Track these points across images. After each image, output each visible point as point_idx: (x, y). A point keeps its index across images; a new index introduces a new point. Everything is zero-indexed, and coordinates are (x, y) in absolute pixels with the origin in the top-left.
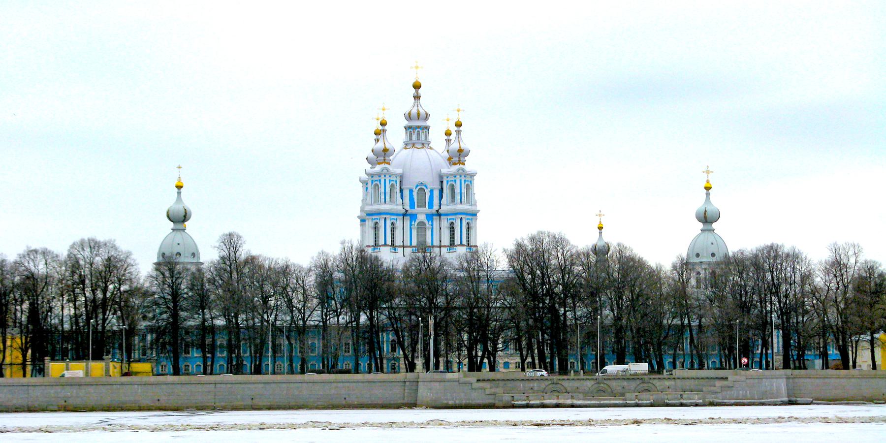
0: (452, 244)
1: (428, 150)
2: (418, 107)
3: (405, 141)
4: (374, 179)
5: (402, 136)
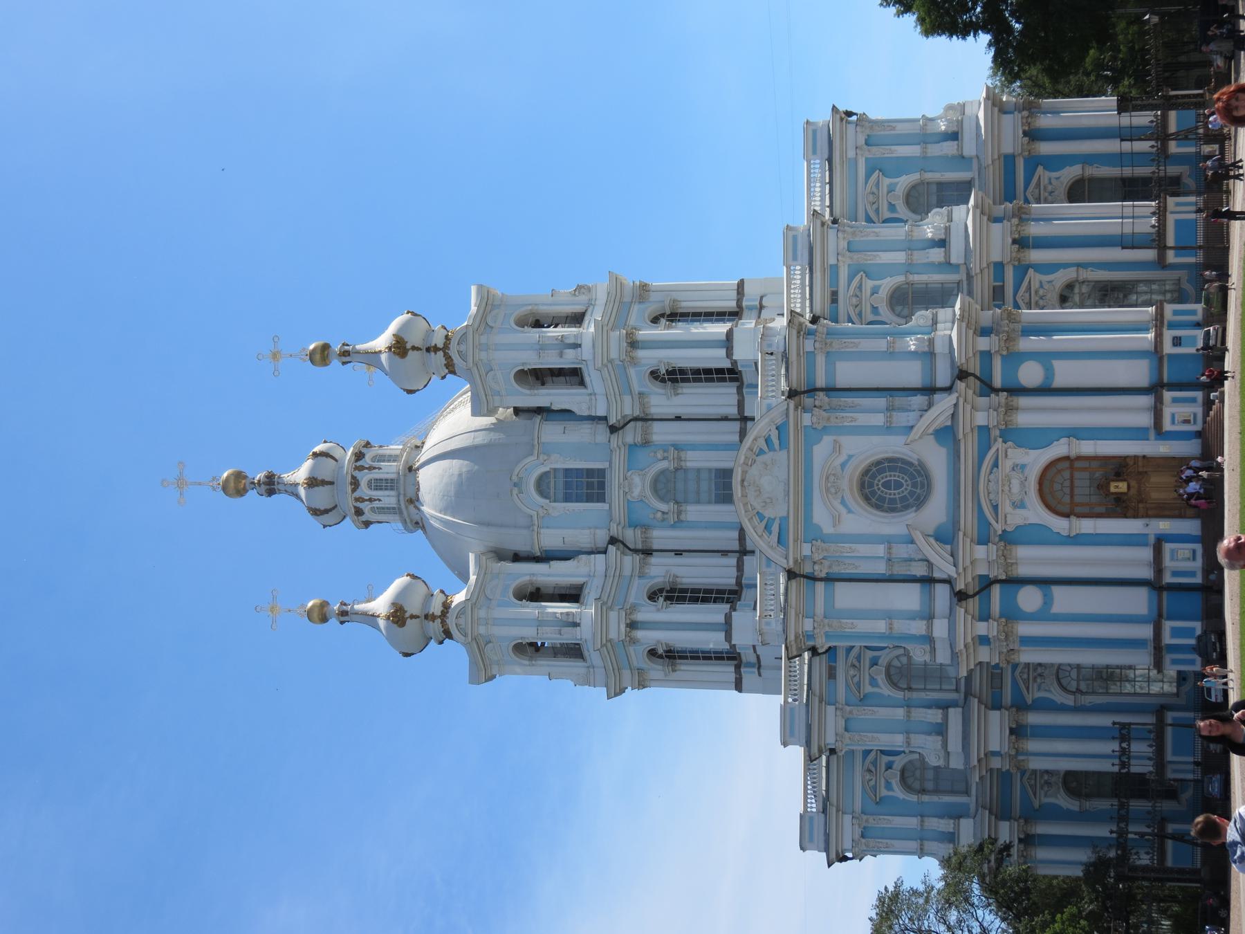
1: (424, 455)
3: (400, 526)
5: (388, 532)
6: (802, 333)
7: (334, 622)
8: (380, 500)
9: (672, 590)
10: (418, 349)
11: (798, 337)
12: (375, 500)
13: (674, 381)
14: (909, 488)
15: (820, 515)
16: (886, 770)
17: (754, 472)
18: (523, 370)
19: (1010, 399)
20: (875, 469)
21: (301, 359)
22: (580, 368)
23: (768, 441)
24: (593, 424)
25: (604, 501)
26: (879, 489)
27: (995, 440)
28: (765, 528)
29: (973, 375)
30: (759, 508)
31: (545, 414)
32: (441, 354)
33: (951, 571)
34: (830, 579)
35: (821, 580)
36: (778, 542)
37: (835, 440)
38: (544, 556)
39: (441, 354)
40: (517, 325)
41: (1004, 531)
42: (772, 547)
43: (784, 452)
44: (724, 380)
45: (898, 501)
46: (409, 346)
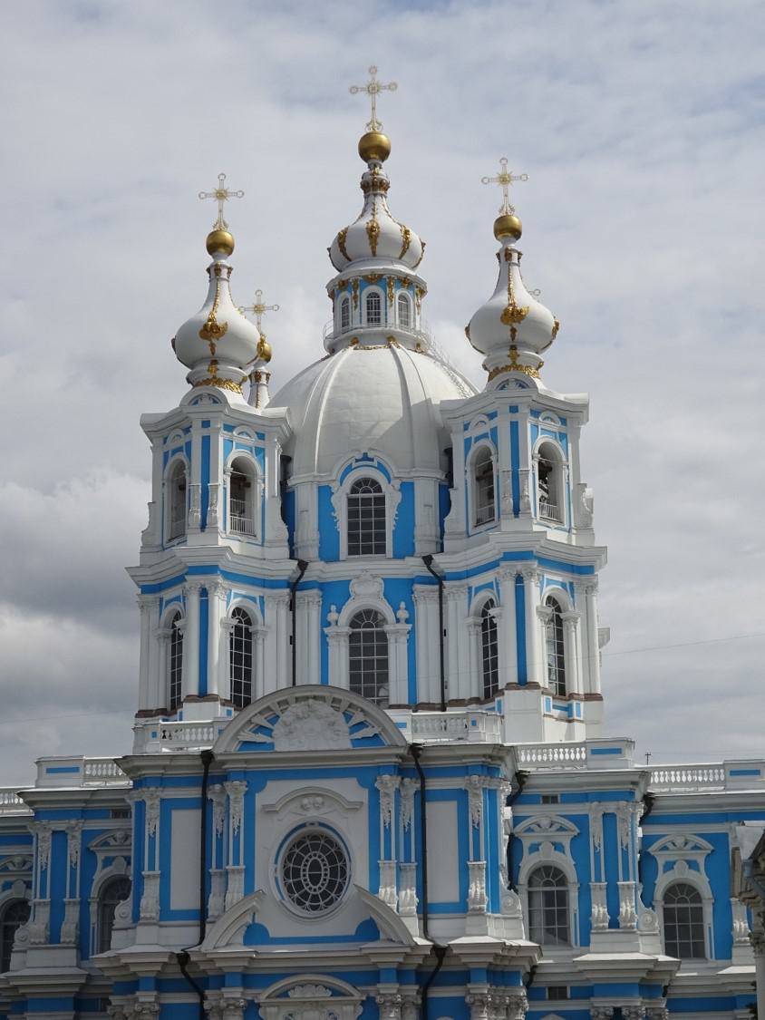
0: (491, 691)
2: (373, 215)
4: (171, 445)
6: (489, 760)
7: (209, 260)
8: (356, 307)
9: (249, 635)
10: (513, 337)
11: (484, 756)
12: (356, 302)
13: (484, 626)
14: (312, 892)
15: (273, 792)
16: (25, 882)
17: (325, 709)
18: (491, 454)
19: (414, 1011)
20: (333, 850)
21: (503, 208)
22: (493, 520)
23: (361, 725)
24: (436, 536)
25: (349, 554)
26: (310, 857)
27: (362, 992)
28: (261, 726)
29: (440, 964)
30: (283, 717)
31: (446, 483)
32: (509, 362)
33: (207, 946)
34: (205, 805)
35: (204, 793)
36: (246, 743)
37: (362, 803)
38: (288, 490)
39: (509, 362)
40: (542, 445)
41: (258, 1006)
42: (237, 733)
43: (349, 746)
44: (487, 682)
45: (295, 880)
46: (515, 325)
